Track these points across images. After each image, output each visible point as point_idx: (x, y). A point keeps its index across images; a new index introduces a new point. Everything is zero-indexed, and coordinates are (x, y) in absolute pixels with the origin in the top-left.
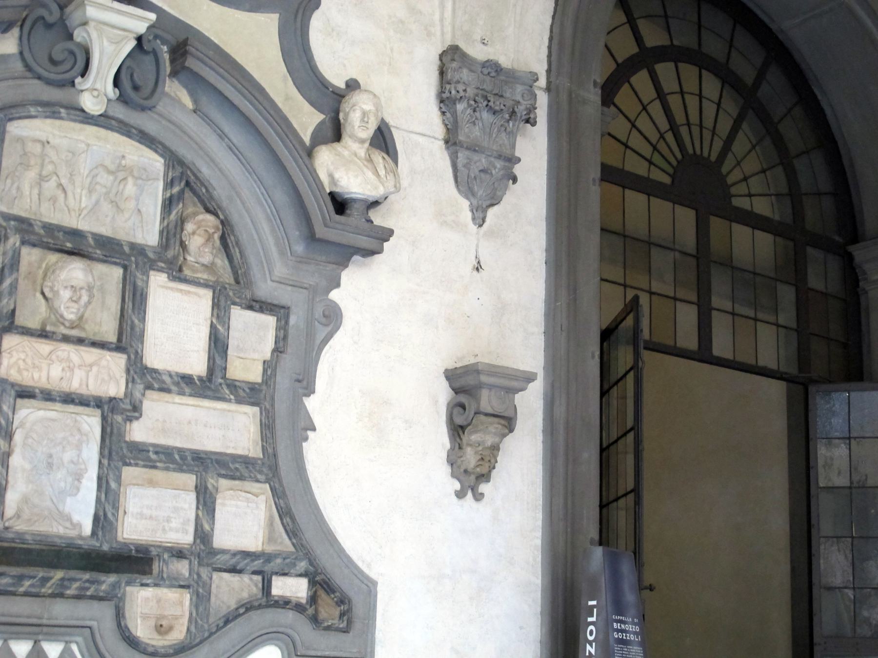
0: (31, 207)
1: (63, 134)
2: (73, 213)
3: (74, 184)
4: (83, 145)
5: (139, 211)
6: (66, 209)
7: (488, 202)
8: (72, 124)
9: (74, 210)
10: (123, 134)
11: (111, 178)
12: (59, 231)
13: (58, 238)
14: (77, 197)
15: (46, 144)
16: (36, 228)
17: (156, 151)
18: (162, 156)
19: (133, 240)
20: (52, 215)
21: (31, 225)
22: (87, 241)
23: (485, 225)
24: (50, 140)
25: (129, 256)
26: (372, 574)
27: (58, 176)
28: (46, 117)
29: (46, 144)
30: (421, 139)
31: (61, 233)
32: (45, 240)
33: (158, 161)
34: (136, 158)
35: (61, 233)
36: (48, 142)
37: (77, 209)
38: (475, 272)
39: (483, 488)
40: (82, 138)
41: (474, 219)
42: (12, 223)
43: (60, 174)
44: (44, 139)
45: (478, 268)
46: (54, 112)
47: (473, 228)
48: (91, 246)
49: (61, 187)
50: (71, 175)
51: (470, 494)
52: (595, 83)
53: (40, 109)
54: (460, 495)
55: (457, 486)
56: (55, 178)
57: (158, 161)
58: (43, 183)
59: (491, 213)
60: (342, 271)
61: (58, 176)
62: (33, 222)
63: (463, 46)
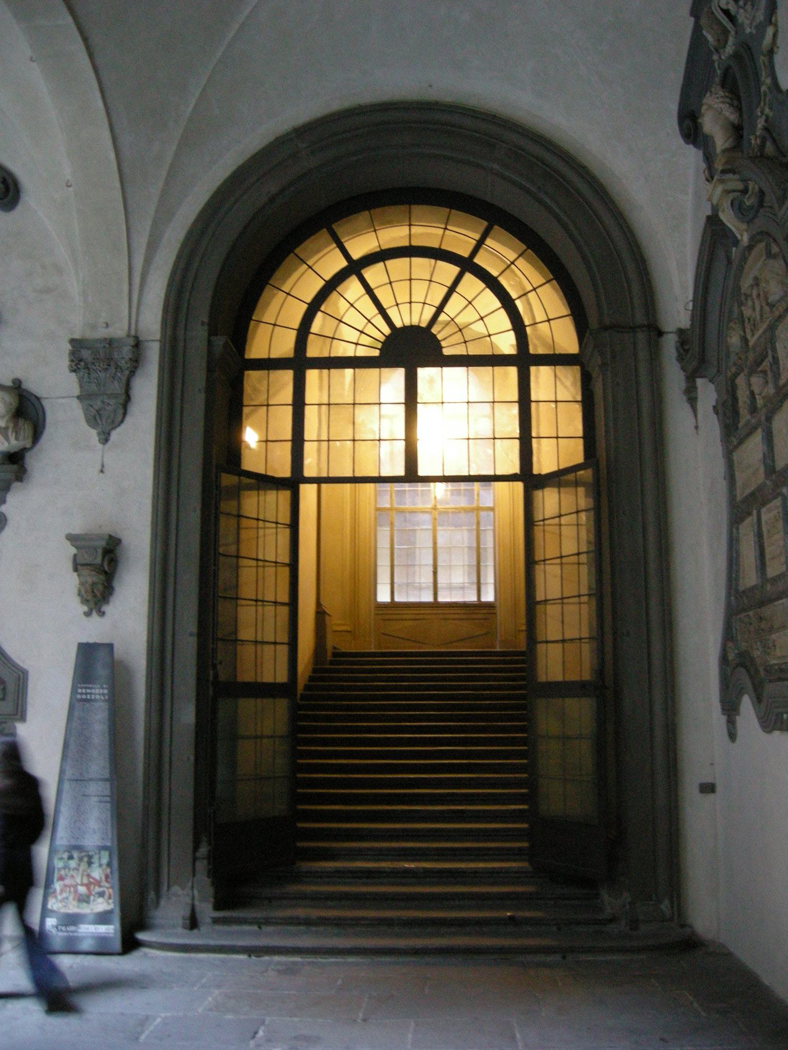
7: (110, 427)
23: (109, 443)
26: (25, 666)
30: (64, 401)
38: (101, 474)
39: (105, 608)
41: (99, 441)
45: (102, 471)
47: (100, 446)
51: (94, 613)
52: (203, 323)
54: (88, 614)
55: (86, 609)
59: (114, 435)
60: (6, 493)
63: (90, 335)
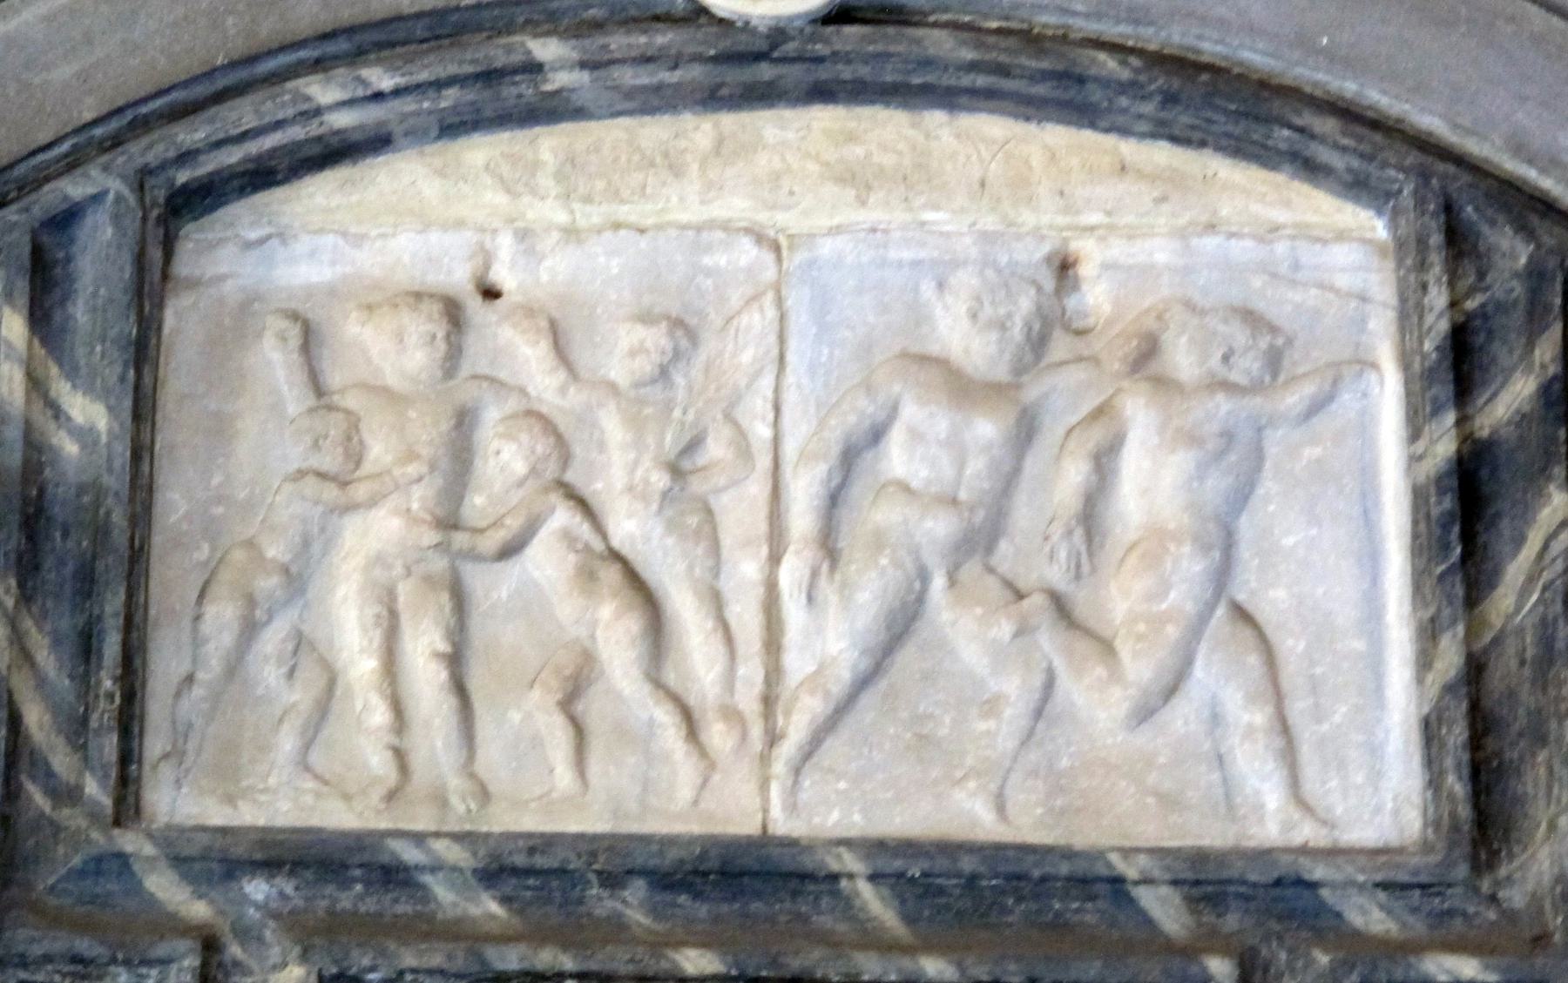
0: (400, 757)
1: (590, 216)
2: (718, 736)
3: (709, 533)
4: (747, 252)
5: (1242, 614)
6: (665, 718)
8: (654, 131)
9: (731, 714)
10: (1030, 107)
11: (986, 429)
12: (613, 881)
13: (616, 929)
14: (746, 616)
15: (474, 305)
16: (443, 893)
17: (1311, 169)
18: (1357, 187)
19: (1213, 835)
20: (564, 777)
21: (394, 876)
22: (847, 906)
24: (503, 276)
25: (1189, 951)
27: (583, 505)
28: (454, 127)
29: (474, 305)
31: (637, 890)
32: (510, 959)
33: (1341, 236)
34: (1161, 252)
35: (637, 890)
36: (491, 293)
37: (748, 700)
40: (737, 206)
42: (257, 889)
43: (595, 489)
44: (459, 277)
46: (490, 77)
48: (886, 946)
49: (611, 575)
50: (676, 471)
53: (383, 80)
56: (563, 516)
57: (1341, 236)
58: (478, 578)
61: (583, 505)
62: (410, 854)
